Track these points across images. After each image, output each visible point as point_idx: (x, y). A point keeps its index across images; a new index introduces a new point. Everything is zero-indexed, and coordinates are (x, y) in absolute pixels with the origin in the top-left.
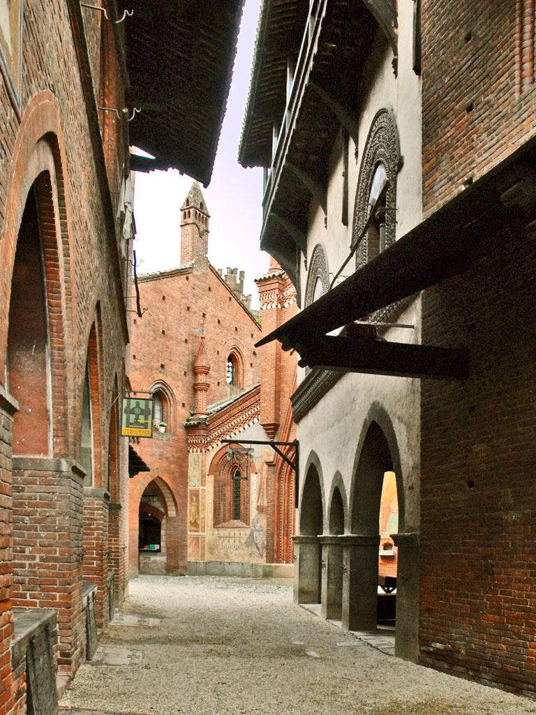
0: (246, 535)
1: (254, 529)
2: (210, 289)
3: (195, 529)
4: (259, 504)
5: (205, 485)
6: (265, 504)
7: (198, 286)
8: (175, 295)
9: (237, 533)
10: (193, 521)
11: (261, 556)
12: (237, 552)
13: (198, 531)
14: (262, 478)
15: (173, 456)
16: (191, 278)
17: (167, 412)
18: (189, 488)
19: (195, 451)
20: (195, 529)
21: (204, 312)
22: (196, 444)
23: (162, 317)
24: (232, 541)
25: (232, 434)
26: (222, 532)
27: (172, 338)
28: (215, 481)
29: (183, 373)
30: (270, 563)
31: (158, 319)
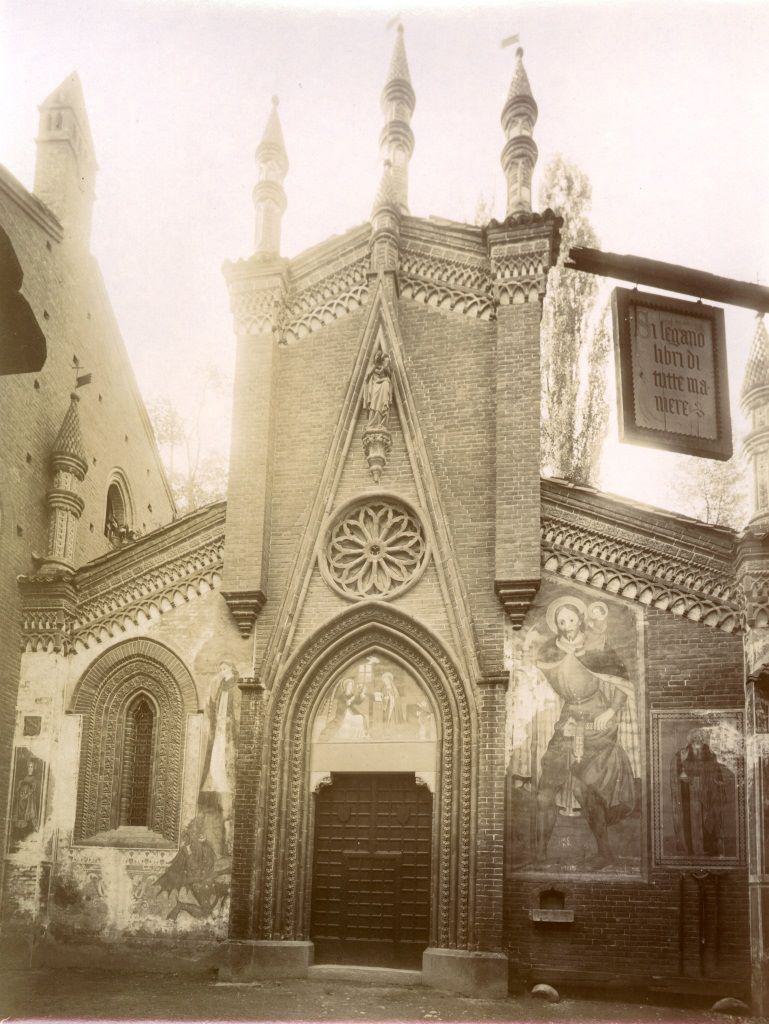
28: (87, 725)
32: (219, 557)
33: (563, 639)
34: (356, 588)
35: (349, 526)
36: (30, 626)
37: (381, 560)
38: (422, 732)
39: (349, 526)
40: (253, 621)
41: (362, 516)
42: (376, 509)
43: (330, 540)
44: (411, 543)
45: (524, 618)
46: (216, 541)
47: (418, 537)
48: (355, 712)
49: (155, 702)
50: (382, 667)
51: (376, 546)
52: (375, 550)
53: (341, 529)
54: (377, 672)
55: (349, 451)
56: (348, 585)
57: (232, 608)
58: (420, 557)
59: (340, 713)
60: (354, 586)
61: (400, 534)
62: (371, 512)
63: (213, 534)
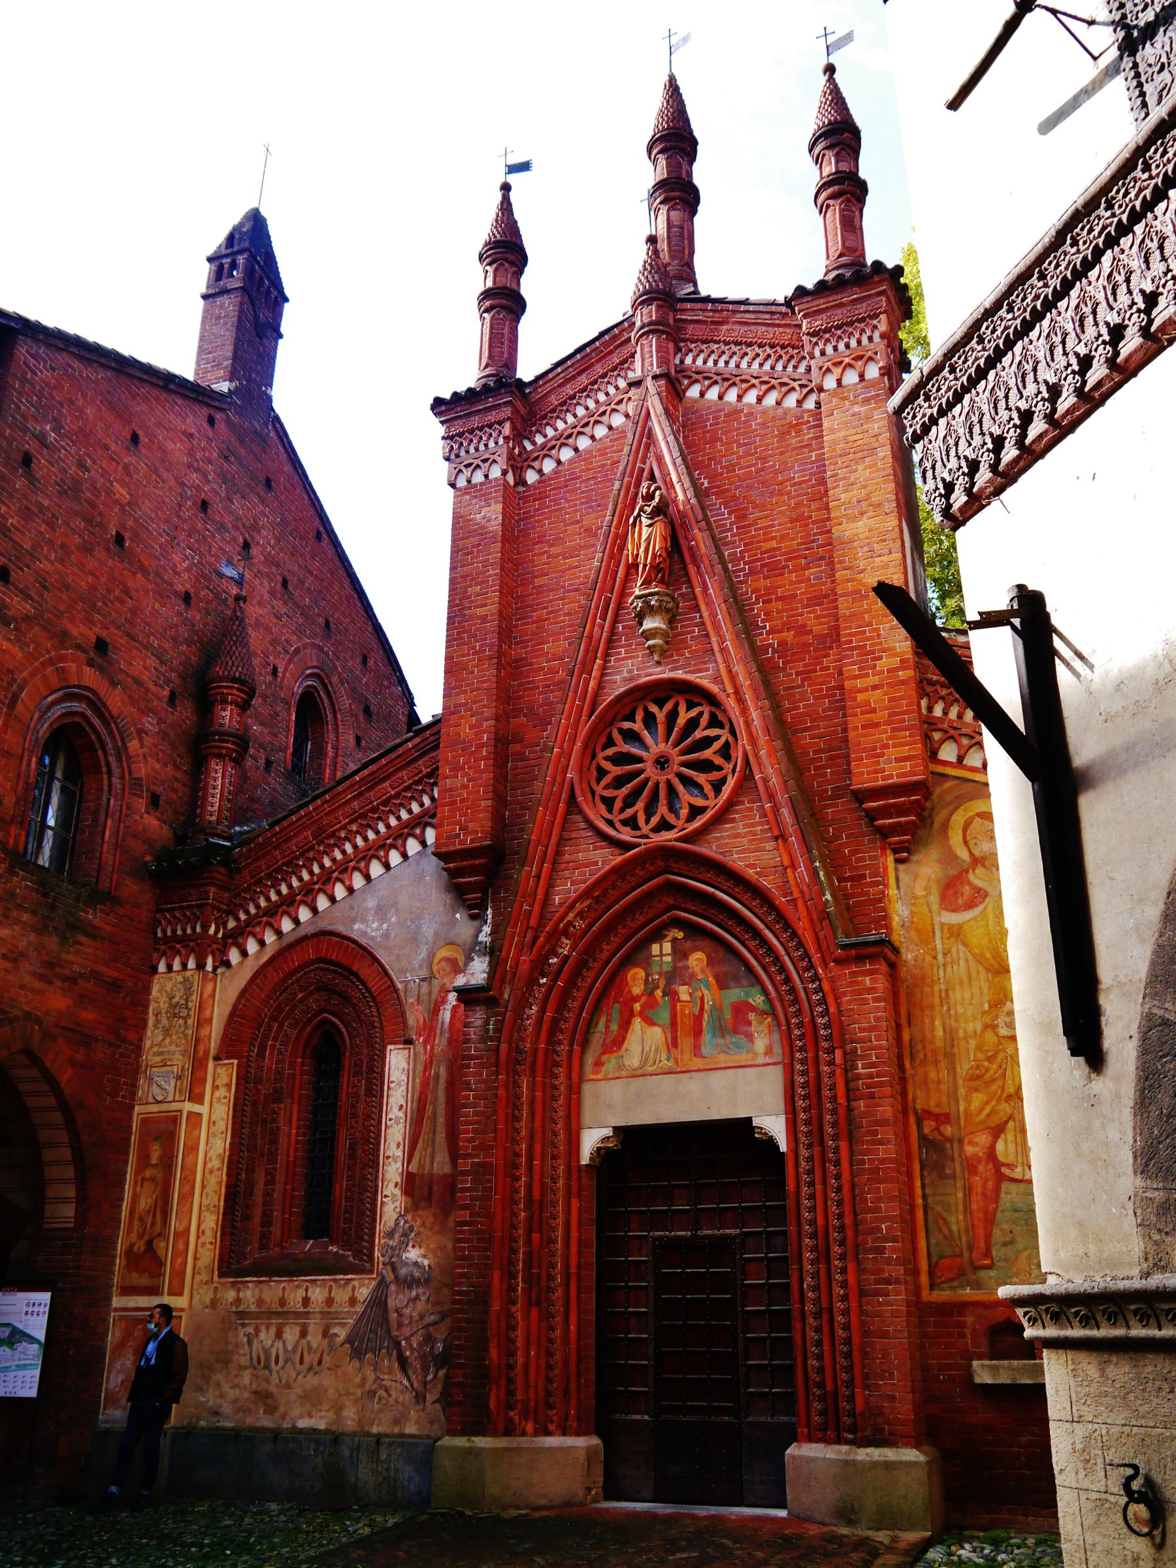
0: (353, 1301)
1: (390, 1277)
2: (268, 483)
3: (144, 1281)
4: (413, 1168)
5: (199, 1099)
6: (441, 1164)
7: (238, 458)
8: (170, 446)
9: (317, 1295)
10: (140, 1246)
11: (420, 1398)
12: (312, 1381)
13: (155, 1291)
14: (427, 1066)
15: (95, 975)
16: (221, 426)
17: (96, 813)
18: (137, 1109)
19: (177, 965)
20: (144, 1281)
21: (249, 539)
22: (184, 940)
23: (121, 492)
24: (291, 1334)
25: (322, 903)
26: (250, 1294)
27: (144, 570)
28: (243, 1079)
29: (166, 693)
30: (465, 1432)
31: (109, 492)
32: (432, 799)
33: (980, 870)
34: (636, 827)
35: (621, 731)
36: (164, 932)
37: (671, 777)
38: (760, 1044)
39: (621, 731)
40: (485, 893)
41: (639, 716)
42: (661, 705)
43: (594, 756)
44: (717, 745)
45: (908, 841)
46: (429, 775)
47: (725, 735)
48: (650, 1022)
49: (344, 1030)
50: (688, 944)
51: (662, 757)
52: (662, 762)
53: (610, 737)
54: (680, 953)
55: (615, 621)
56: (625, 823)
57: (452, 873)
58: (731, 766)
59: (626, 1025)
60: (632, 823)
61: (698, 734)
62: (654, 708)
63: (423, 767)
